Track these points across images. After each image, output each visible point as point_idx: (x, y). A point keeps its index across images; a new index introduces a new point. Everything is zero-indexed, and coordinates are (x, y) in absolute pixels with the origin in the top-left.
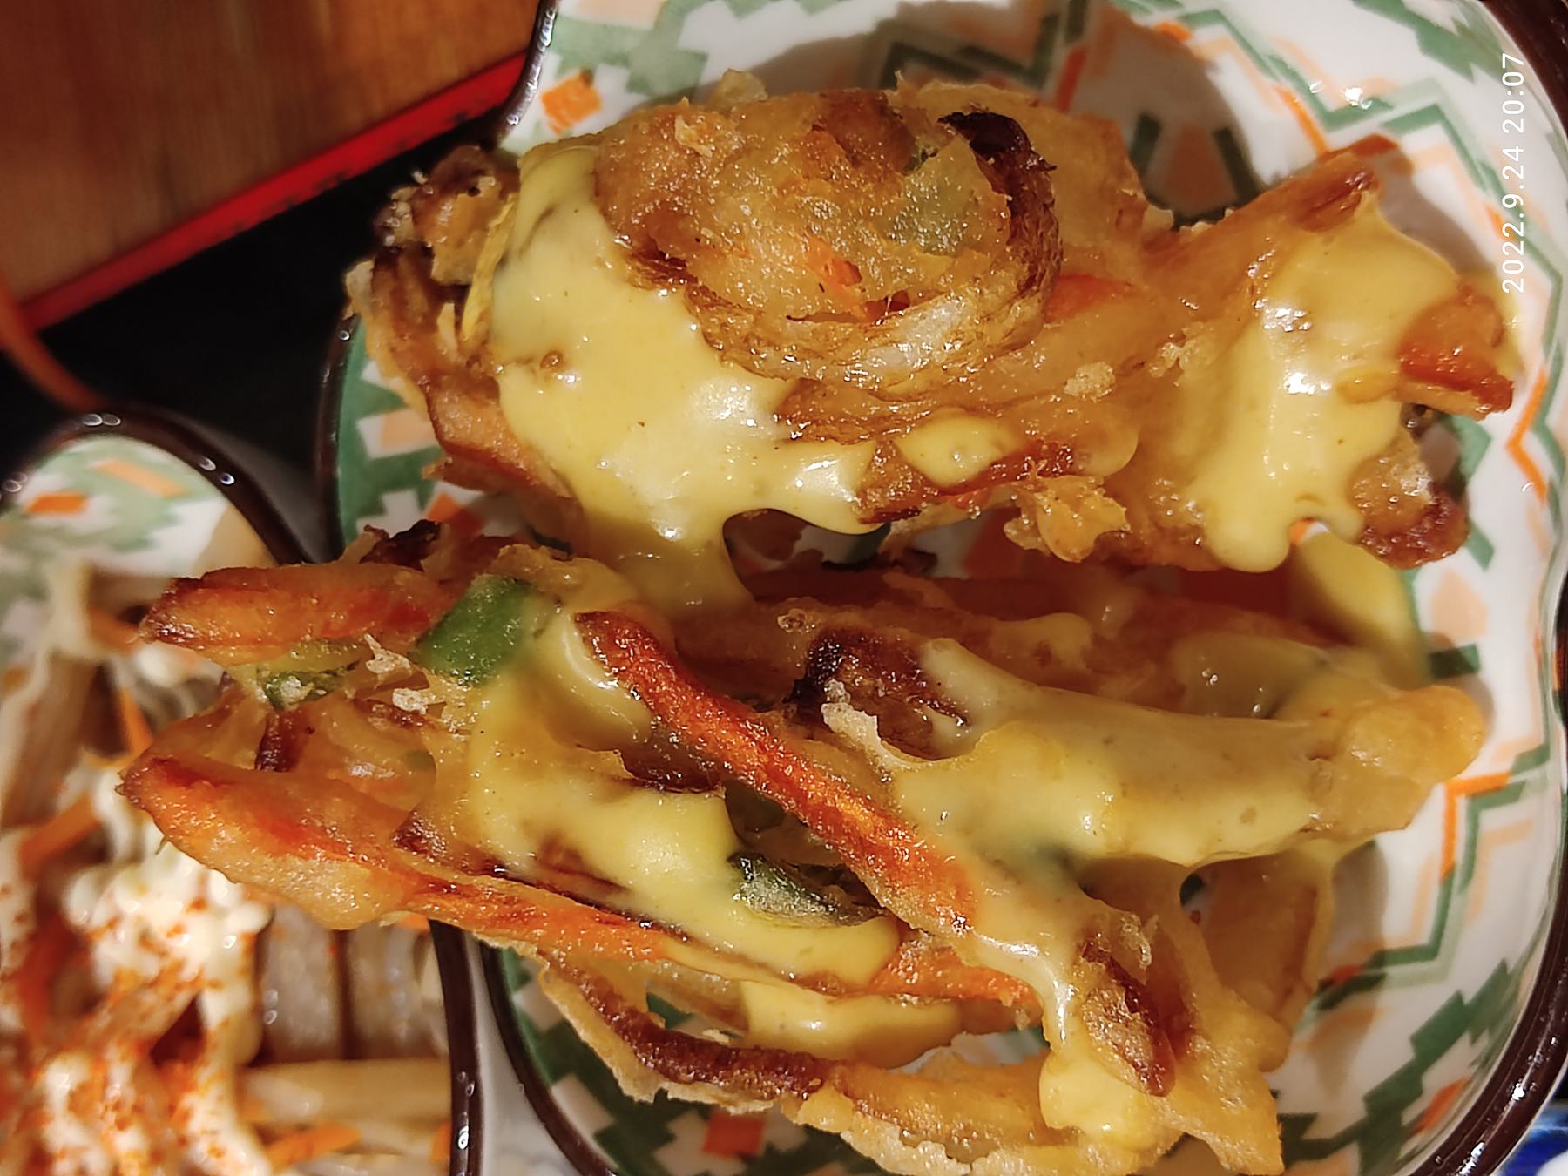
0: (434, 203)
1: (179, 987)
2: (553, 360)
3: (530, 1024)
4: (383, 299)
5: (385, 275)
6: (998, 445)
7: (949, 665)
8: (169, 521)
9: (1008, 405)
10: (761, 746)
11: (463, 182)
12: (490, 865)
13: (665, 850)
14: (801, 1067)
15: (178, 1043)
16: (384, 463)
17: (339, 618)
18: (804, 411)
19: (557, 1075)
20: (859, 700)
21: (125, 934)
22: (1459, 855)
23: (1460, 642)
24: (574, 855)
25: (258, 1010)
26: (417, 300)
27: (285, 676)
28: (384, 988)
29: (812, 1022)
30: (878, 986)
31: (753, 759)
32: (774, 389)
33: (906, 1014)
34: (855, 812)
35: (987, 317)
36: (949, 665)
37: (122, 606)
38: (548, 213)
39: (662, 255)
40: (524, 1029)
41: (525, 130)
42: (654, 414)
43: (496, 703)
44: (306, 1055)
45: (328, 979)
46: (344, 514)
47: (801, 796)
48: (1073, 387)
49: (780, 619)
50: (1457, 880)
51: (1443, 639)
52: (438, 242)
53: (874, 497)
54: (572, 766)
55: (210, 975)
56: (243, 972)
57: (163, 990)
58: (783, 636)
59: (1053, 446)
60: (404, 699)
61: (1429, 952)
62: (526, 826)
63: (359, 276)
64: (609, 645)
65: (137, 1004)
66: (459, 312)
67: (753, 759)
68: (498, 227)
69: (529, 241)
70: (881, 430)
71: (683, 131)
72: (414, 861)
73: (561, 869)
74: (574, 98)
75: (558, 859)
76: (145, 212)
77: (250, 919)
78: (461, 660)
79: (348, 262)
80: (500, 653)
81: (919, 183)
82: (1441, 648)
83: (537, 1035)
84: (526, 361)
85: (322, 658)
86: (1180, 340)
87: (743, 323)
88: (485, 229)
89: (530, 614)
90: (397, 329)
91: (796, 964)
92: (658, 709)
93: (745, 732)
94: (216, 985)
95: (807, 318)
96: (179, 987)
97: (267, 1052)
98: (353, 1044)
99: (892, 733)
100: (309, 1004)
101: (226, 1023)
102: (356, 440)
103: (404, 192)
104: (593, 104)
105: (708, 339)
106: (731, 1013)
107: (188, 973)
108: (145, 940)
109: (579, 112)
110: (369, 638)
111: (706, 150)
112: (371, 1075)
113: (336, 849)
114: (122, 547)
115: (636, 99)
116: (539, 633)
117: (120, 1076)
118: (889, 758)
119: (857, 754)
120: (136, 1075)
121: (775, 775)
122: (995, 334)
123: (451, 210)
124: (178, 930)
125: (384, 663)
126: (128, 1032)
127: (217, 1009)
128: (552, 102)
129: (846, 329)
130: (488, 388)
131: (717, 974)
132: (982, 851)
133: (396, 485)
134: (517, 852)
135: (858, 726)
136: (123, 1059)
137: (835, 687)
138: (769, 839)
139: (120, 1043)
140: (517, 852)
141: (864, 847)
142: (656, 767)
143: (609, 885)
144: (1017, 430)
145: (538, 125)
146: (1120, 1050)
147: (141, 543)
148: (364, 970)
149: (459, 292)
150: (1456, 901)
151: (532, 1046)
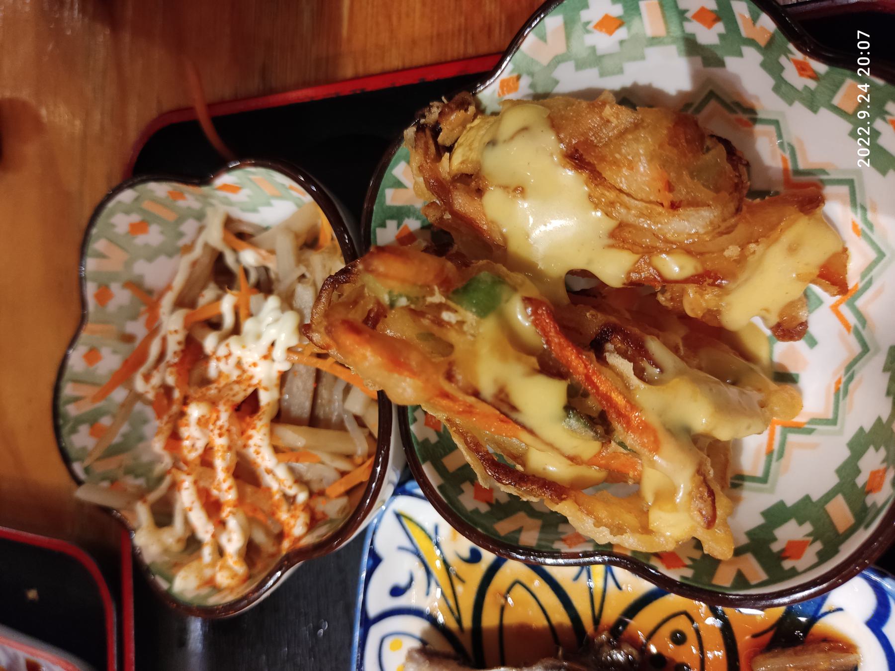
0: (452, 111)
1: (249, 386)
2: (519, 190)
3: (416, 438)
4: (421, 144)
5: (421, 134)
6: (696, 268)
7: (655, 346)
8: (269, 204)
9: (702, 254)
10: (586, 366)
11: (463, 105)
12: (476, 394)
13: (540, 399)
14: (558, 489)
15: (248, 406)
16: (390, 208)
17: (431, 277)
18: (620, 236)
19: (424, 461)
20: (624, 355)
21: (232, 361)
22: (776, 446)
23: (792, 370)
24: (507, 396)
25: (280, 401)
26: (432, 149)
27: (401, 295)
28: (330, 401)
29: (554, 467)
30: (590, 463)
31: (581, 369)
32: (611, 224)
33: (594, 473)
34: (619, 399)
35: (724, 220)
36: (655, 346)
37: (239, 234)
38: (525, 129)
39: (577, 158)
40: (413, 440)
41: (489, 92)
42: (552, 221)
43: (489, 327)
44: (295, 422)
45: (311, 395)
46: (373, 224)
47: (597, 388)
48: (727, 253)
49: (588, 314)
50: (775, 456)
51: (781, 366)
52: (445, 127)
53: (634, 276)
54: (519, 359)
55: (263, 384)
56: (276, 385)
57: (243, 387)
58: (595, 321)
59: (716, 274)
60: (446, 316)
61: (764, 480)
62: (496, 381)
63: (410, 132)
64: (535, 312)
65: (231, 389)
66: (450, 158)
67: (581, 369)
68: (471, 128)
69: (512, 138)
70: (650, 251)
71: (608, 111)
72: (448, 387)
73: (502, 400)
74: (511, 84)
75: (502, 396)
76: (254, 84)
77: (285, 367)
78: (476, 305)
79: (407, 127)
80: (489, 307)
81: (708, 157)
82: (781, 371)
83: (418, 443)
84: (505, 188)
85: (415, 292)
86: (757, 242)
87: (611, 195)
88: (464, 127)
89: (504, 292)
90: (425, 157)
91: (571, 452)
92: (548, 342)
93: (581, 359)
94: (266, 389)
95: (642, 200)
96: (249, 386)
97: (281, 417)
98: (314, 421)
99: (639, 373)
100: (300, 403)
101: (268, 404)
102: (384, 196)
103: (436, 104)
104: (516, 89)
105: (590, 196)
106: (521, 458)
107: (255, 381)
108: (239, 365)
109: (510, 90)
110: (436, 288)
111: (614, 122)
112: (323, 434)
113: (414, 374)
114: (244, 210)
115: (530, 91)
116: (507, 301)
117: (224, 416)
118: (635, 381)
119: (620, 375)
120: (230, 417)
121: (588, 378)
122: (724, 226)
123: (456, 117)
124: (255, 365)
125: (437, 298)
126: (228, 400)
127: (265, 398)
128: (504, 84)
129: (660, 209)
130: (480, 192)
131: (520, 441)
132: (664, 425)
133: (392, 218)
134: (487, 388)
135: (625, 366)
136: (226, 411)
137: (609, 346)
138: (575, 402)
139: (225, 404)
140: (487, 388)
141: (620, 414)
142: (549, 367)
143: (514, 408)
144: (703, 263)
145: (494, 91)
146: (700, 511)
147: (255, 210)
148: (324, 393)
149: (450, 149)
150: (774, 464)
151: (416, 448)
